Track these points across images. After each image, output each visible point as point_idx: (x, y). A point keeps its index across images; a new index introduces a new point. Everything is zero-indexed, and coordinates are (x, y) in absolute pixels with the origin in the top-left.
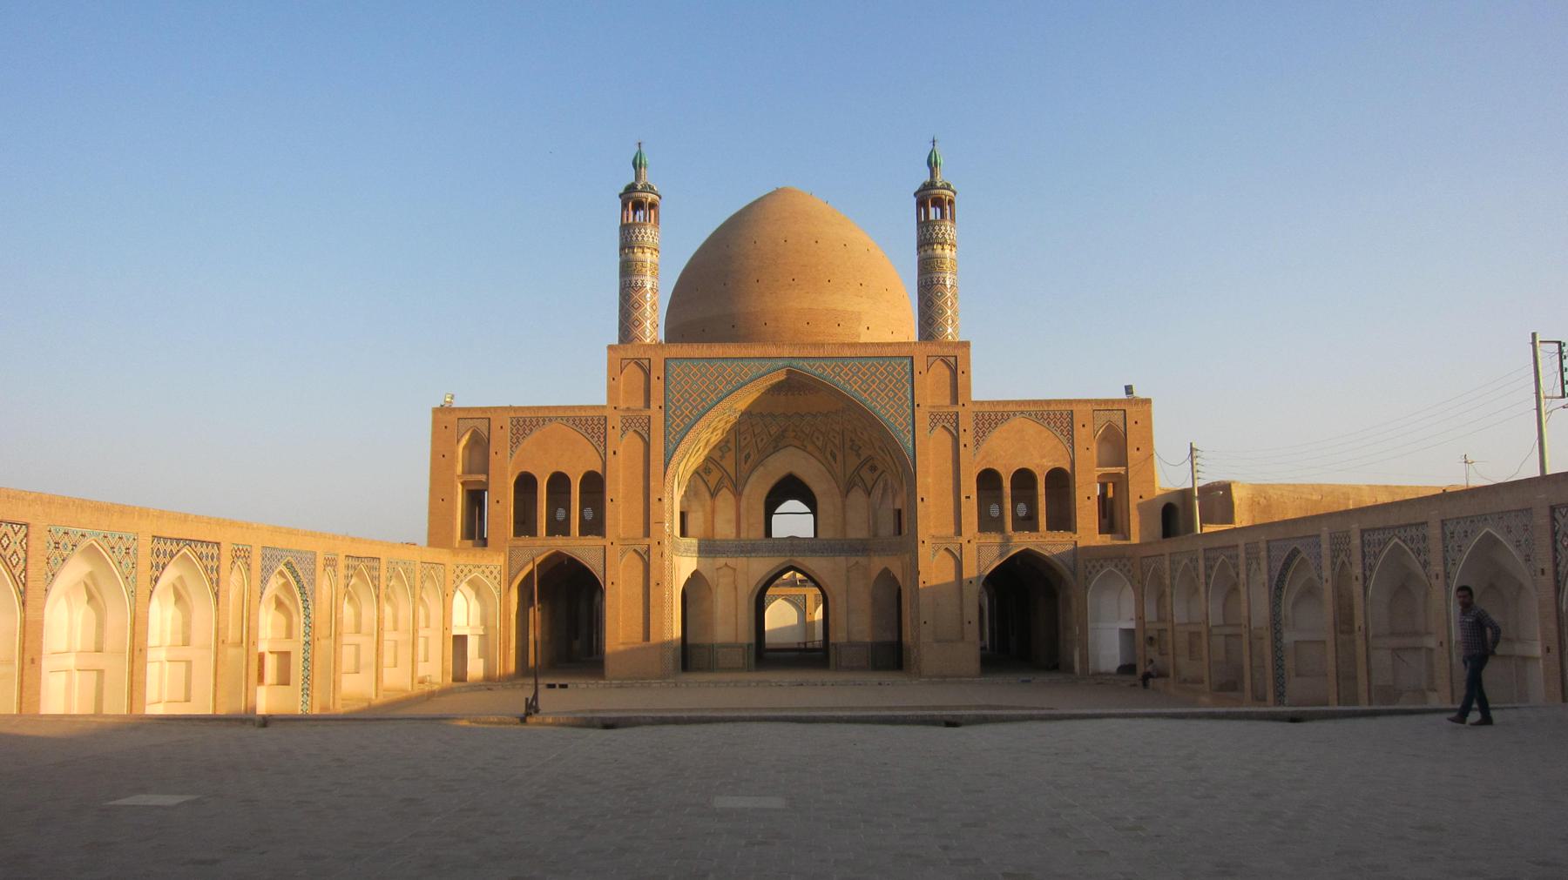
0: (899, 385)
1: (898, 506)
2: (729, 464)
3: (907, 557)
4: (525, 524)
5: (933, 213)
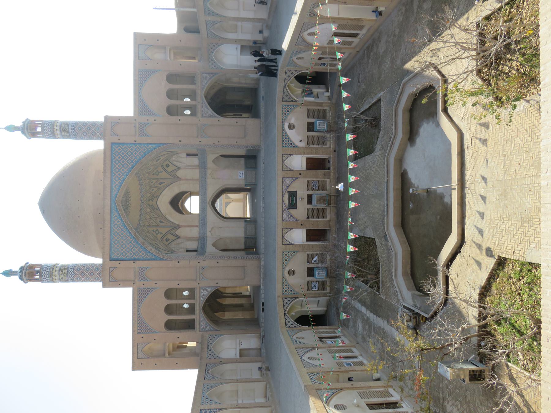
0: (125, 150)
1: (184, 155)
4: (189, 325)
5: (39, 130)
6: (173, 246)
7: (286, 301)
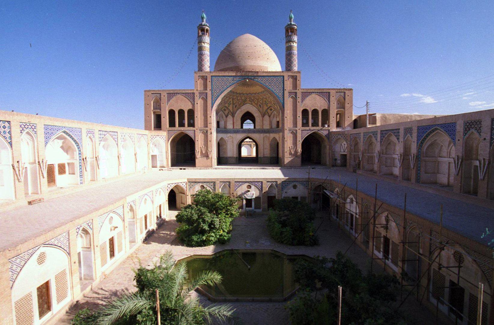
2: (231, 108)
3: (281, 134)
4: (172, 124)
6: (221, 112)
7: (184, 184)
